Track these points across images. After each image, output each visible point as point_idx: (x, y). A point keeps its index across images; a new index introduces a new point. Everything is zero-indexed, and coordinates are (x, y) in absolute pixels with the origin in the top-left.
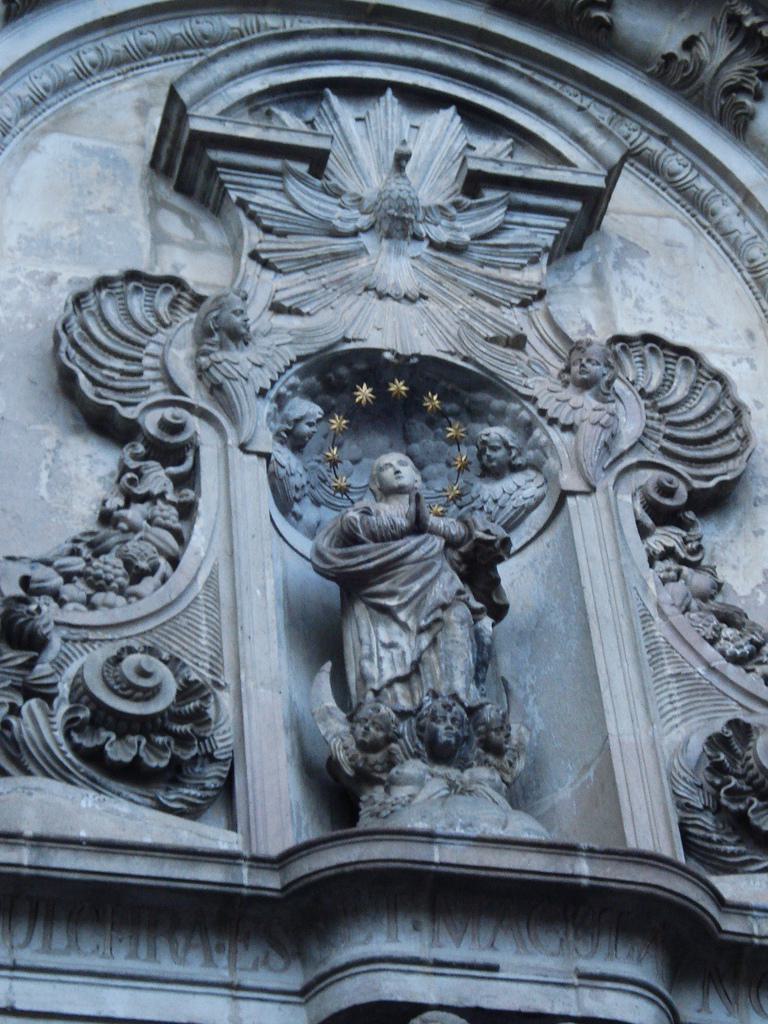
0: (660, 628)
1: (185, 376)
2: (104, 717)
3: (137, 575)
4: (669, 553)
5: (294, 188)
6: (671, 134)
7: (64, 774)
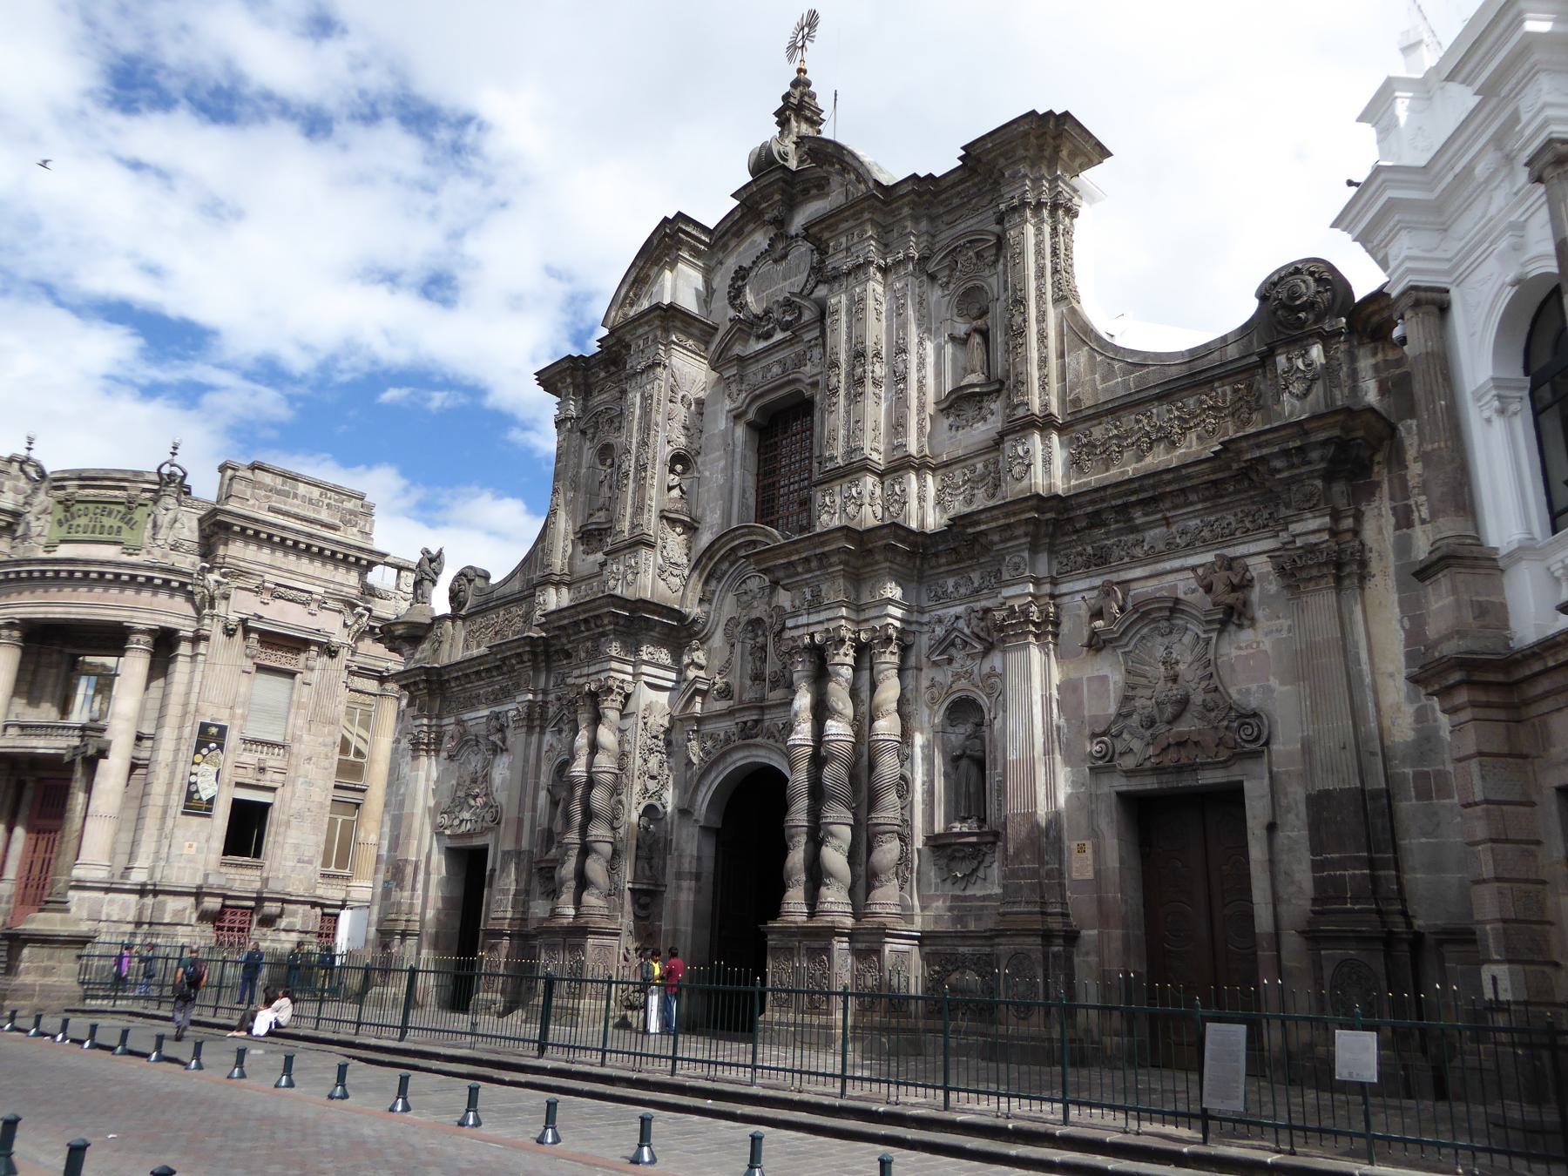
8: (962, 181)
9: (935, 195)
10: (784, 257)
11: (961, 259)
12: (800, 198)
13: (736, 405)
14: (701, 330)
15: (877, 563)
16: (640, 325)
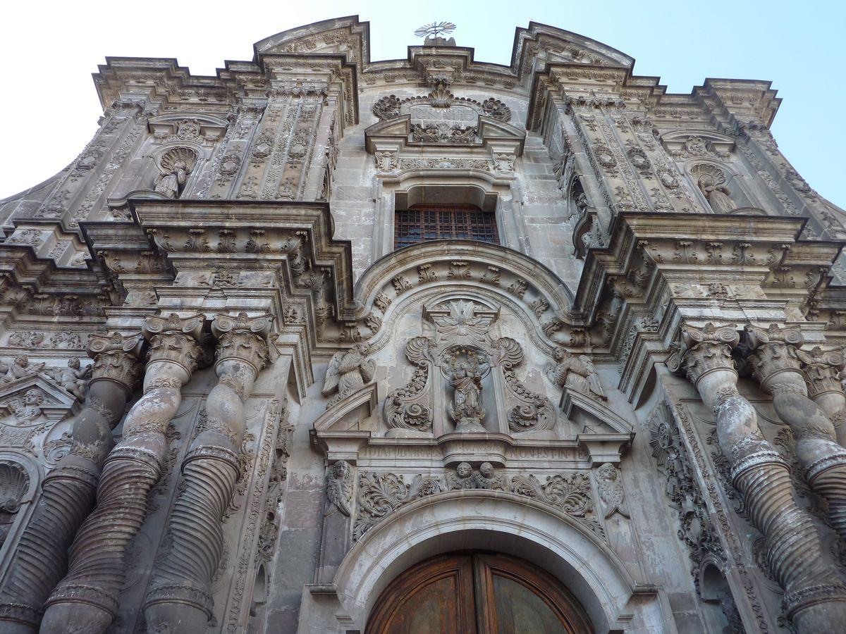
0: (507, 390)
1: (426, 353)
2: (410, 416)
3: (417, 390)
4: (509, 376)
5: (445, 318)
6: (510, 301)
7: (403, 427)
8: (677, 105)
9: (659, 104)
10: (447, 106)
11: (689, 145)
12: (464, 82)
13: (390, 173)
14: (349, 112)
15: (793, 286)
16: (303, 65)
